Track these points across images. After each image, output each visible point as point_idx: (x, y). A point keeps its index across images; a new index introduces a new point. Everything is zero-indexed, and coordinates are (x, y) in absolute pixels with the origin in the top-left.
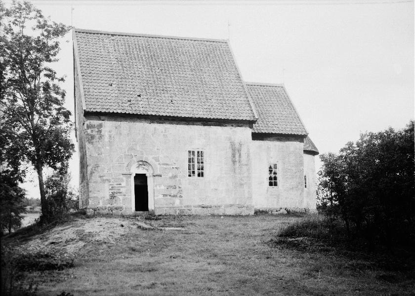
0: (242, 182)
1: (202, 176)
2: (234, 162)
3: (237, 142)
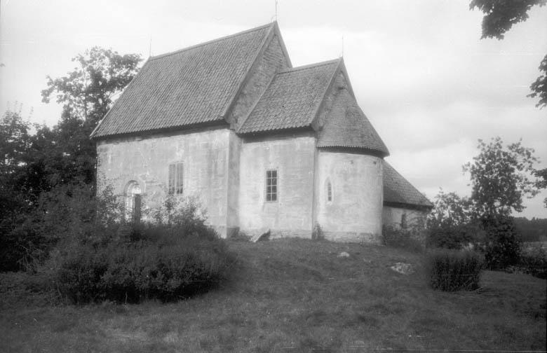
0: (218, 198)
1: (181, 192)
2: (210, 173)
3: (214, 148)
